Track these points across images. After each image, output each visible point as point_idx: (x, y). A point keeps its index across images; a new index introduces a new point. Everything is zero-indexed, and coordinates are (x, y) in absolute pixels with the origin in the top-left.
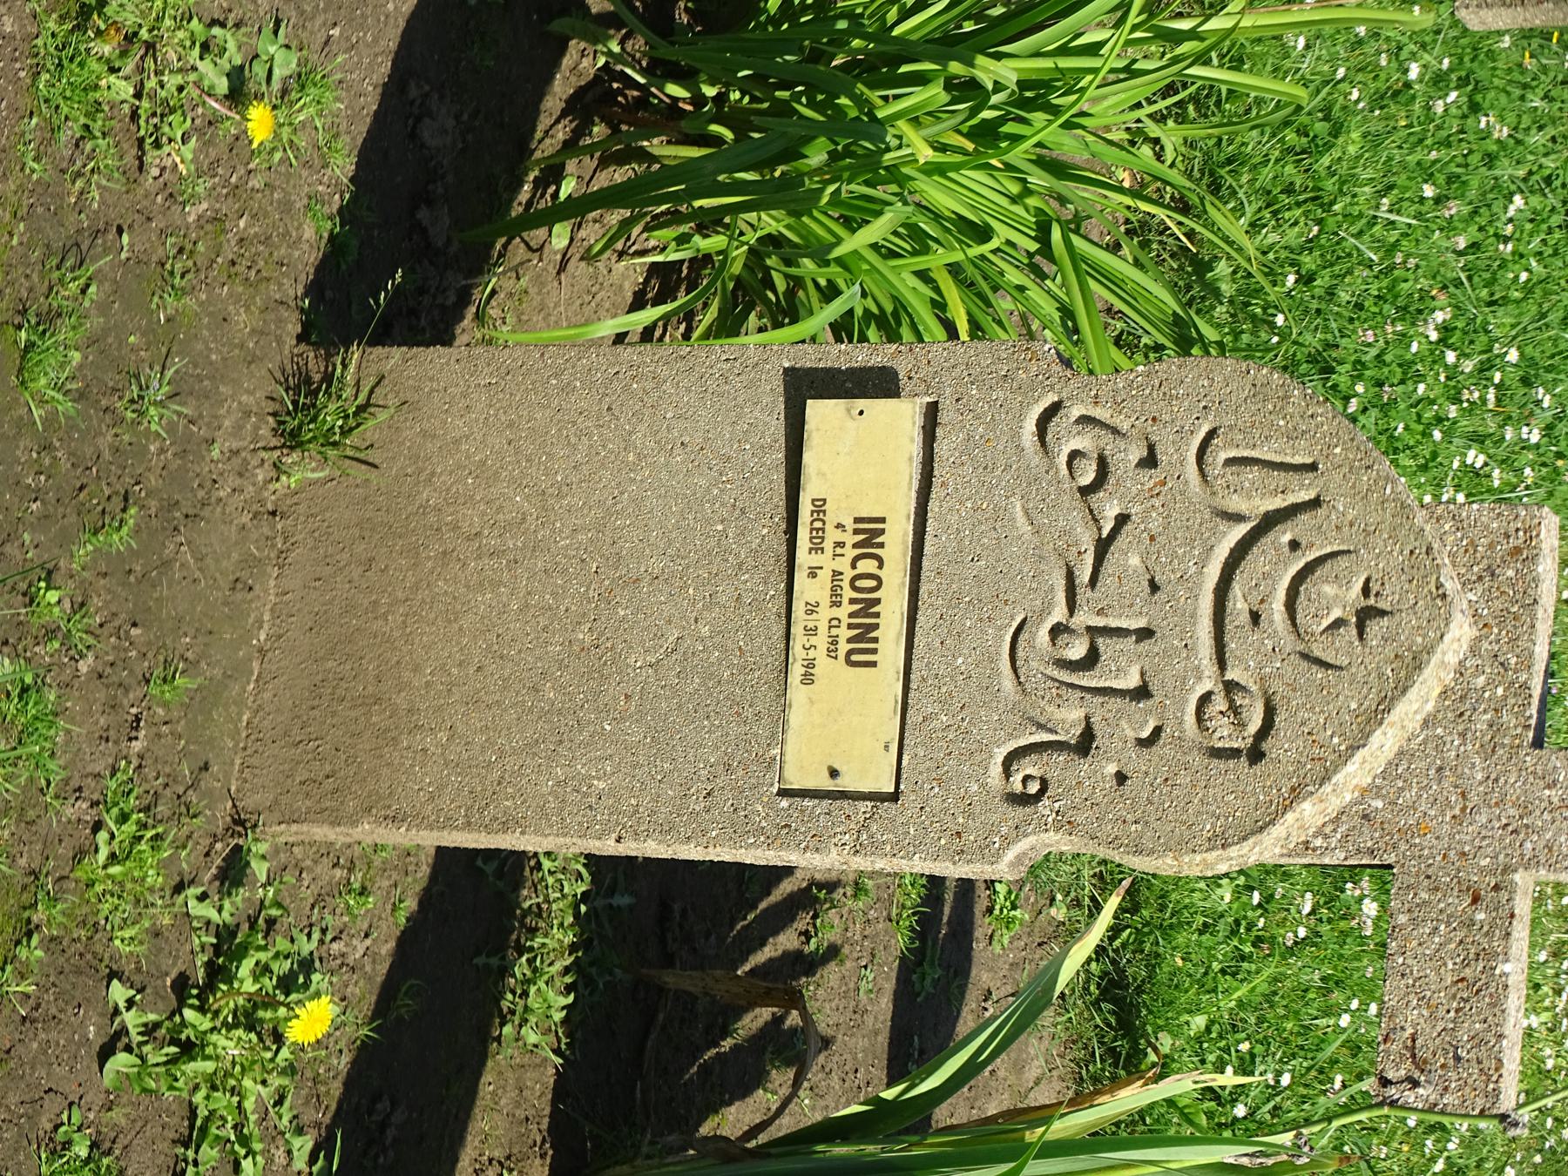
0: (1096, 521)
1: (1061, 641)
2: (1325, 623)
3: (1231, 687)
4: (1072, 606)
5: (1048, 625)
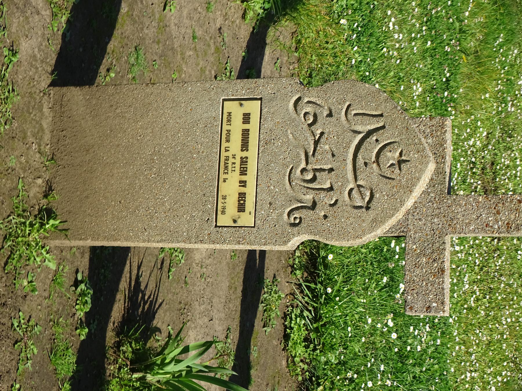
0: (314, 135)
1: (304, 173)
2: (389, 165)
3: (359, 186)
4: (307, 163)
5: (300, 169)
